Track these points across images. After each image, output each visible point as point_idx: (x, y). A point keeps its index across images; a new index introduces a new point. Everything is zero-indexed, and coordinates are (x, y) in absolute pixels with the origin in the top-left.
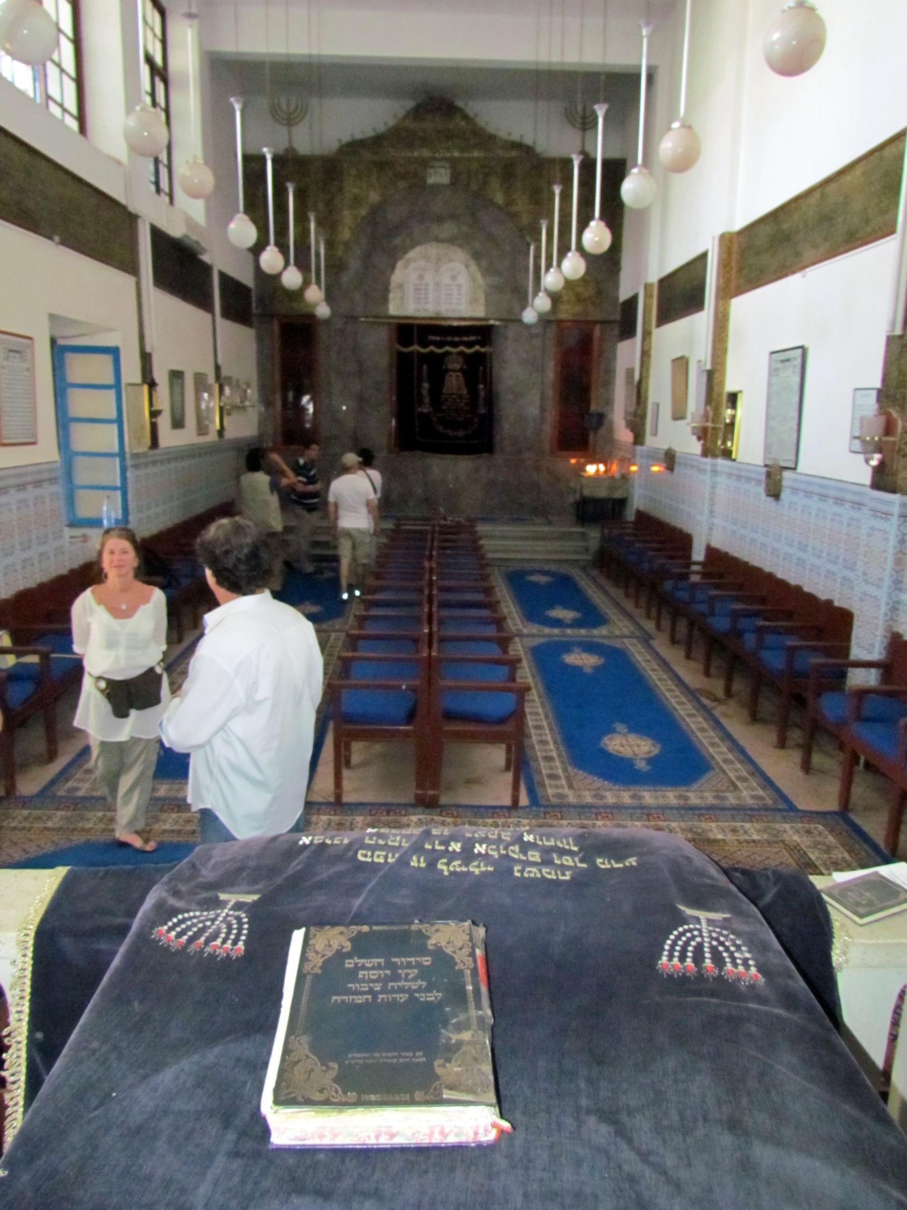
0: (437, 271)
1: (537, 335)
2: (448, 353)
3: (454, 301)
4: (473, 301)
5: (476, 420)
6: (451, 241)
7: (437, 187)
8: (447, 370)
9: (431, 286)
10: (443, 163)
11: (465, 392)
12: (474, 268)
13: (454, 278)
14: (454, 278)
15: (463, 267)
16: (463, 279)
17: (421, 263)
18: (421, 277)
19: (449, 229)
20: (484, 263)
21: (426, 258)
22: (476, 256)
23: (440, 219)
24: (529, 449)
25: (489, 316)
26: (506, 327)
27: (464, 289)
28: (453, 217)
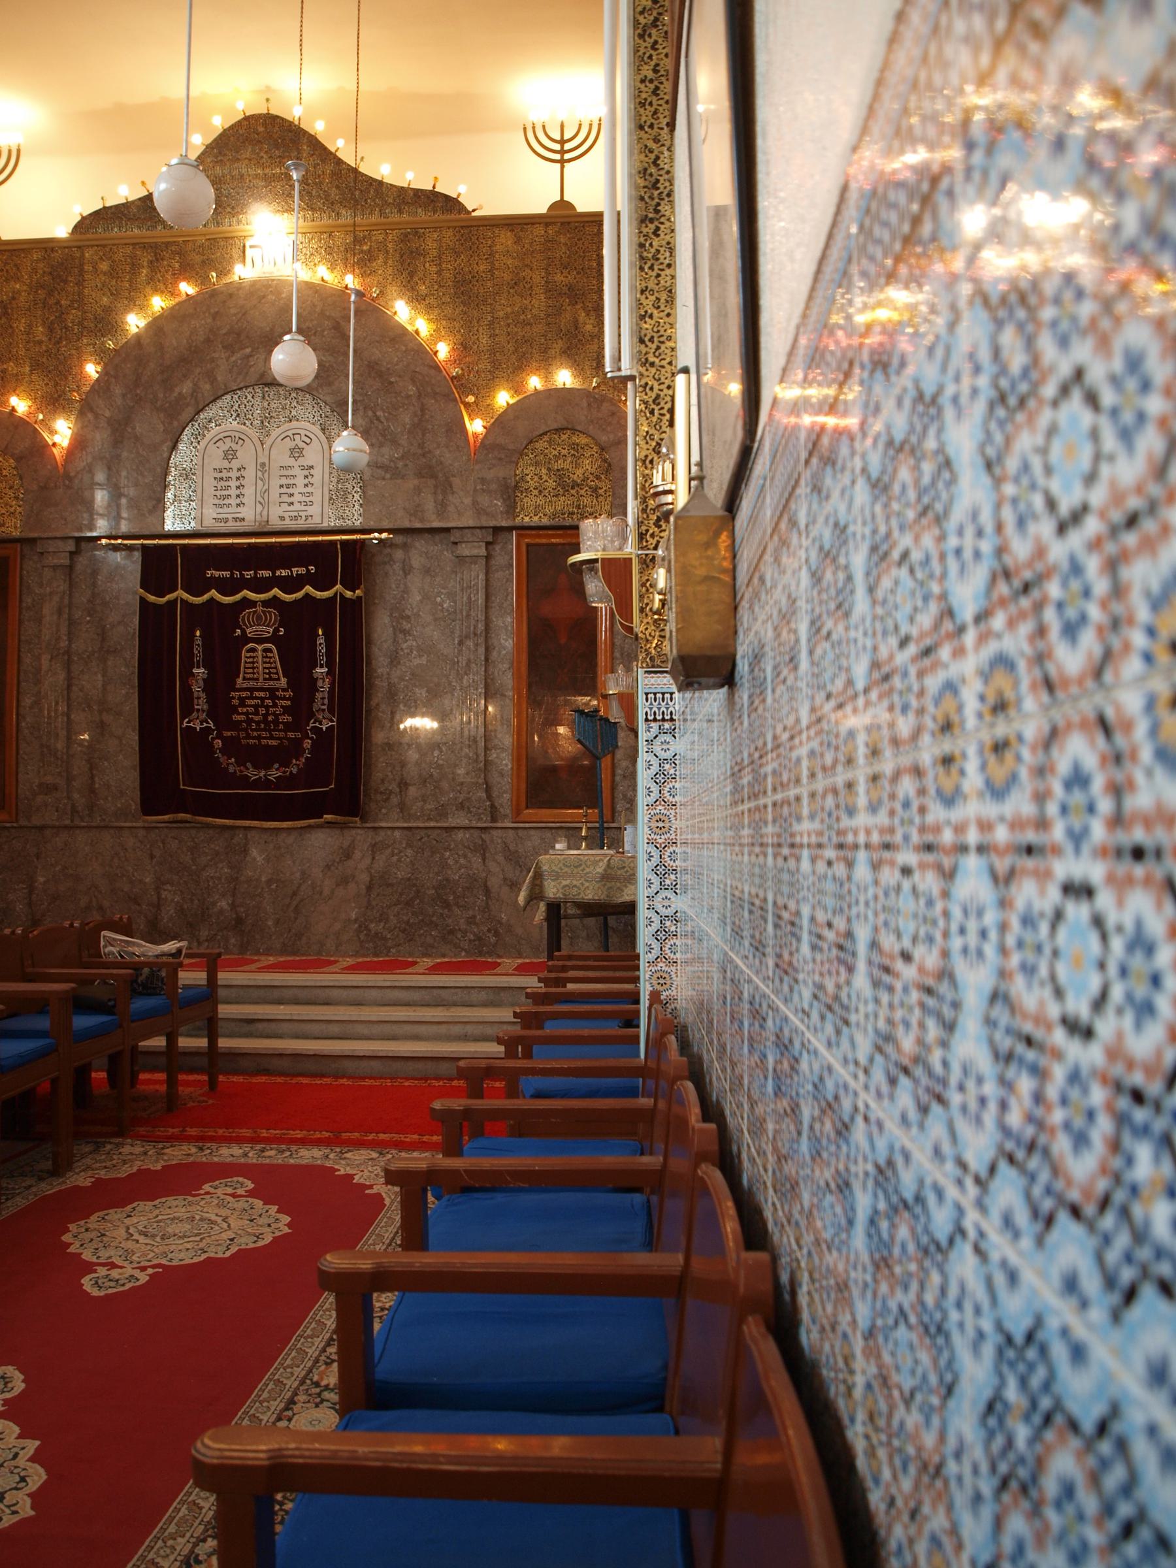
25: (372, 524)
27: (317, 472)
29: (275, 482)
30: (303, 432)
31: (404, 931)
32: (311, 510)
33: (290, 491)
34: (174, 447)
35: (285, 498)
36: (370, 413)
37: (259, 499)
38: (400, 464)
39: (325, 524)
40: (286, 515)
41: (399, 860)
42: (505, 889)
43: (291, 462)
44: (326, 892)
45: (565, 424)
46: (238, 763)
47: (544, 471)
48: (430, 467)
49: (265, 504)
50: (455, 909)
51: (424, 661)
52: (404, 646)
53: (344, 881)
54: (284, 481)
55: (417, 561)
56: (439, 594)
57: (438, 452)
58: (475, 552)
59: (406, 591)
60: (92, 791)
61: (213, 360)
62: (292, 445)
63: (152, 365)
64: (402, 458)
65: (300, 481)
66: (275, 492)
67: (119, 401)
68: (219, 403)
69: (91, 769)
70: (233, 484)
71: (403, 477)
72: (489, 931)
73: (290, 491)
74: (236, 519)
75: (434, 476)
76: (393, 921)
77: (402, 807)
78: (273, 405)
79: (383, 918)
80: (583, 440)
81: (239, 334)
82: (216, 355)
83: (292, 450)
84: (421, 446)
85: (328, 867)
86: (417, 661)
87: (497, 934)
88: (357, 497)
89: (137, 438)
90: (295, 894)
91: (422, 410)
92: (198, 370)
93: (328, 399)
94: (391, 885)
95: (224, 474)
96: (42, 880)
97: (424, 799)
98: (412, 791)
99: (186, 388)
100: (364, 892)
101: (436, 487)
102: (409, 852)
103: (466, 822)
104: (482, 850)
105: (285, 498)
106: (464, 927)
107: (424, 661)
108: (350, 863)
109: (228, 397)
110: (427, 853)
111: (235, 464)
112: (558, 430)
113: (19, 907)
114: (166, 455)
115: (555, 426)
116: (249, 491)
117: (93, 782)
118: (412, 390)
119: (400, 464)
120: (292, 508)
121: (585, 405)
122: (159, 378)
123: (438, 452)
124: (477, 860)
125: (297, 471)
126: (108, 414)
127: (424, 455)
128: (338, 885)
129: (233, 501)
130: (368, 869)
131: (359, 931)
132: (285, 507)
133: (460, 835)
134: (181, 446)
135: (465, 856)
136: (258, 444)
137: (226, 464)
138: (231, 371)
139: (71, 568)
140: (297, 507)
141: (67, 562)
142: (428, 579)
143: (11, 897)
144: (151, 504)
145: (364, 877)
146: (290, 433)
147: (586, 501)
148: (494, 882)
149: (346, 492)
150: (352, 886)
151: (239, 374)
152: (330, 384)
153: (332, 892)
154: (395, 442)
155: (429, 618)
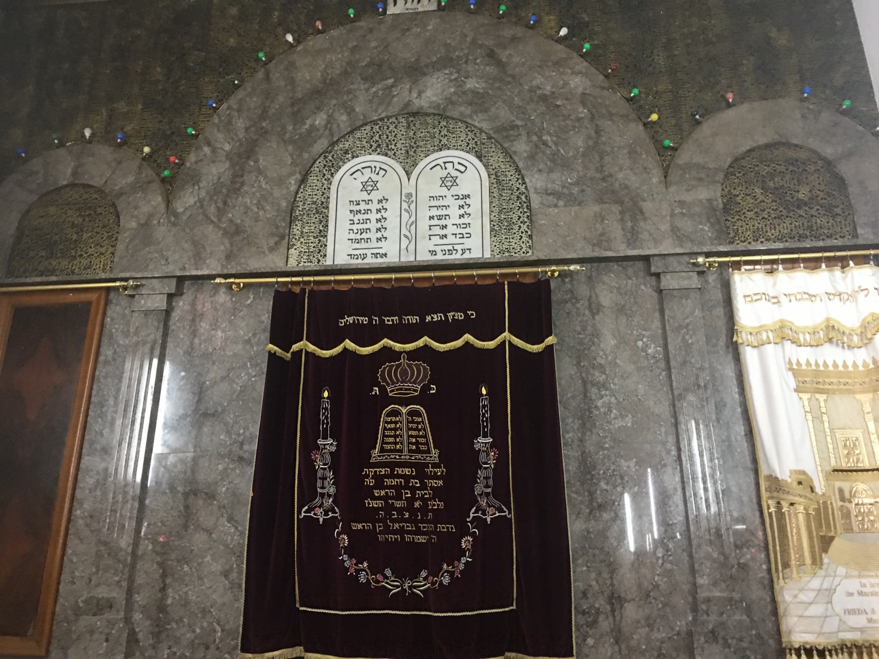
0: (408, 174)
1: (685, 292)
3: (451, 229)
4: (500, 226)
5: (466, 543)
9: (393, 206)
12: (497, 159)
13: (449, 182)
14: (449, 182)
16: (474, 179)
18: (369, 186)
23: (416, 72)
28: (447, 62)
29: (424, 214)
30: (456, 160)
32: (468, 243)
33: (443, 222)
34: (303, 181)
35: (437, 231)
36: (535, 138)
38: (575, 190)
39: (488, 255)
40: (438, 249)
43: (443, 191)
45: (777, 138)
46: (375, 569)
47: (758, 191)
48: (613, 192)
49: (414, 239)
51: (628, 421)
52: (599, 403)
54: (435, 212)
55: (606, 298)
56: (640, 337)
57: (620, 176)
58: (685, 283)
59: (596, 334)
60: (162, 608)
61: (349, 92)
62: (444, 173)
63: (281, 99)
64: (577, 184)
65: (454, 212)
66: (424, 224)
68: (358, 134)
69: (164, 576)
70: (374, 216)
71: (579, 204)
73: (443, 222)
74: (376, 255)
78: (419, 134)
80: (803, 155)
81: (380, 66)
83: (443, 180)
84: (600, 169)
86: (619, 423)
88: (524, 227)
89: (260, 172)
91: (597, 132)
92: (334, 102)
93: (485, 126)
95: (363, 207)
98: (631, 611)
99: (320, 120)
101: (622, 213)
105: (437, 231)
107: (628, 421)
109: (368, 128)
111: (375, 196)
112: (768, 146)
114: (293, 188)
115: (763, 141)
116: (392, 223)
117: (164, 597)
118: (583, 112)
119: (575, 190)
120: (445, 241)
121: (799, 116)
122: (289, 110)
123: (620, 176)
126: (227, 147)
127: (603, 179)
129: (373, 235)
132: (437, 240)
134: (312, 180)
138: (371, 101)
139: (168, 312)
140: (451, 239)
141: (164, 305)
142: (623, 320)
144: (272, 242)
146: (440, 162)
149: (511, 223)
151: (380, 104)
152: (486, 111)
155: (631, 368)
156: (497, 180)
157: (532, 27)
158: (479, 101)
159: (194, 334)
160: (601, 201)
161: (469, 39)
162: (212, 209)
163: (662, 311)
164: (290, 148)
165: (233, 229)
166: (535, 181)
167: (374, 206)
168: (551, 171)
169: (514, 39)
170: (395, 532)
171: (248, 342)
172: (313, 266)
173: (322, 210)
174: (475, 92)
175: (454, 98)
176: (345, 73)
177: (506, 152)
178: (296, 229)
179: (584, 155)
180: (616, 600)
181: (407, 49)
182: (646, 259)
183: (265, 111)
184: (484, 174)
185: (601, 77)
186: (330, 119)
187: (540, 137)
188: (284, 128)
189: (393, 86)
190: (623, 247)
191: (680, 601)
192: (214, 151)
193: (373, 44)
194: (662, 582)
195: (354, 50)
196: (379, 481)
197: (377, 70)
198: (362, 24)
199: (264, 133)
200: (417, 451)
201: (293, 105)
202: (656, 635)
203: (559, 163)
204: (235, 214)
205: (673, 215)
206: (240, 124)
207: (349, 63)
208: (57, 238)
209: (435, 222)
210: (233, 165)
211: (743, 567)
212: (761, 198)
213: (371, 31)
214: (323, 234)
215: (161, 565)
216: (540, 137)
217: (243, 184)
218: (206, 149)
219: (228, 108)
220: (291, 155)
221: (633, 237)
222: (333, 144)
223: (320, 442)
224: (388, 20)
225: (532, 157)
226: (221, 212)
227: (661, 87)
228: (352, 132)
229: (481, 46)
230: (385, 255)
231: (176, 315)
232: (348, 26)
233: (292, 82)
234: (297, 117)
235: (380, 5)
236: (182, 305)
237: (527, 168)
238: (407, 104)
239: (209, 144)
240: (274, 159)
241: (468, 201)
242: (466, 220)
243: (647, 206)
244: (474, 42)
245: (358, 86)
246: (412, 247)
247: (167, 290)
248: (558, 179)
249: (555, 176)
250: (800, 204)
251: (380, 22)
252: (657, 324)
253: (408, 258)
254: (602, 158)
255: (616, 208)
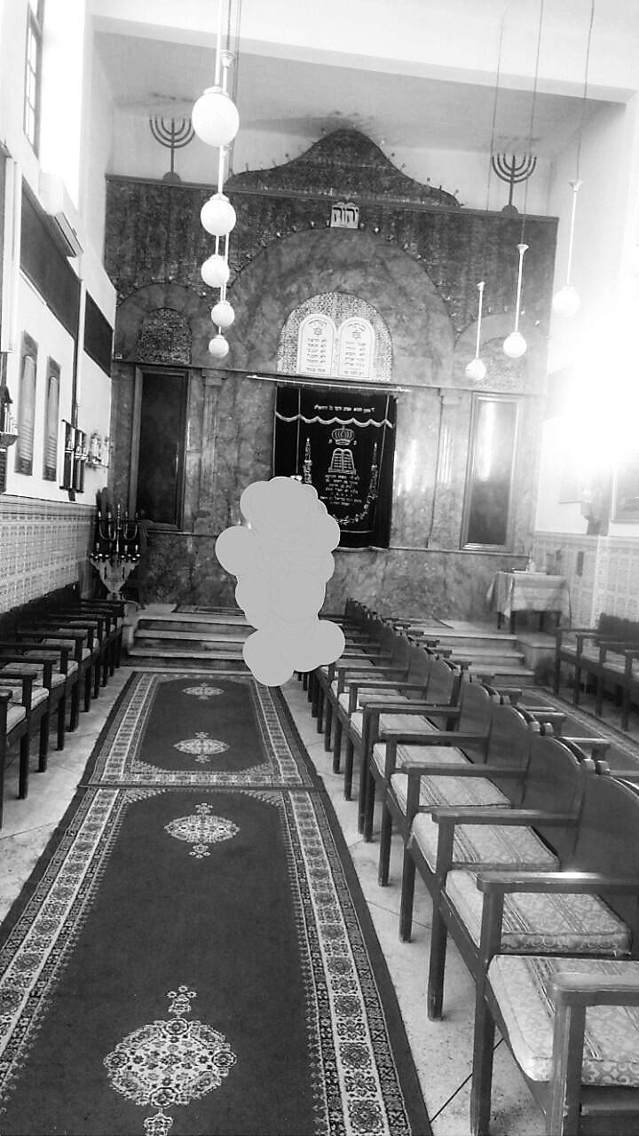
1: (451, 407)
2: (336, 425)
3: (355, 362)
4: (379, 362)
6: (356, 293)
7: (345, 232)
8: (334, 446)
10: (349, 205)
11: (354, 472)
12: (380, 325)
15: (368, 322)
17: (321, 316)
18: (318, 332)
19: (353, 279)
20: (392, 320)
21: (325, 310)
22: (384, 311)
23: (344, 266)
24: (435, 540)
25: (396, 381)
26: (414, 396)
28: (360, 265)
31: (400, 604)
32: (363, 369)
34: (285, 323)
37: (334, 359)
41: (400, 566)
42: (455, 585)
44: (360, 581)
47: (491, 361)
50: (428, 593)
53: (370, 576)
55: (419, 404)
56: (430, 424)
58: (452, 402)
61: (310, 274)
62: (354, 330)
63: (273, 272)
64: (415, 345)
67: (253, 291)
68: (312, 299)
69: (229, 504)
72: (445, 605)
75: (432, 357)
76: (395, 597)
77: (402, 538)
79: (390, 596)
82: (312, 271)
84: (426, 338)
85: (362, 568)
87: (449, 608)
90: (343, 580)
92: (301, 279)
93: (376, 305)
94: (394, 579)
95: (314, 342)
96: (199, 565)
97: (414, 534)
98: (408, 530)
99: (294, 288)
100: (380, 582)
102: (406, 562)
103: (437, 549)
104: (444, 563)
105: (348, 361)
106: (432, 603)
108: (374, 566)
109: (318, 296)
110: (415, 563)
113: (183, 580)
114: (280, 327)
116: (328, 353)
118: (423, 306)
119: (414, 348)
122: (277, 280)
124: (441, 568)
125: (356, 345)
126: (246, 298)
128: (366, 577)
130: (384, 570)
131: (376, 602)
133: (433, 555)
135: (435, 566)
136: (334, 326)
137: (315, 337)
143: (178, 574)
145: (381, 574)
147: (512, 379)
148: (450, 581)
150: (374, 579)
152: (377, 297)
153: (363, 581)
154: (412, 336)
156: (379, 335)
157: (404, 250)
158: (375, 291)
159: (235, 399)
160: (424, 355)
161: (373, 252)
162: (239, 334)
163: (441, 413)
164: (279, 303)
165: (249, 345)
166: (397, 340)
167: (320, 343)
168: (404, 336)
169: (395, 257)
170: (337, 501)
171: (259, 407)
172: (291, 373)
173: (294, 341)
174: (373, 284)
175: (363, 287)
176: (308, 262)
177: (386, 323)
178: (281, 349)
179: (420, 330)
180: (404, 527)
181: (341, 251)
182: (439, 389)
183: (265, 277)
184: (373, 333)
185: (434, 287)
186: (299, 288)
187: (401, 317)
188: (276, 292)
189: (332, 274)
190: (430, 381)
191: (426, 528)
192: (239, 299)
193: (323, 246)
194: (422, 521)
195: (313, 247)
196: (332, 481)
197: (324, 263)
198: (317, 231)
199: (265, 292)
200: (347, 469)
201: (280, 277)
202: (416, 539)
203: (408, 332)
204: (251, 337)
205: (454, 368)
206: (253, 285)
207: (310, 255)
208: (160, 338)
209: (348, 356)
210: (249, 310)
211: (450, 517)
212: (492, 364)
213: (322, 237)
214: (294, 355)
215: (227, 500)
216: (401, 317)
217: (255, 320)
218: (235, 298)
219: (246, 274)
220: (279, 307)
221: (435, 377)
222: (301, 303)
223: (306, 461)
224: (332, 230)
225: (396, 327)
226: (244, 335)
227: (460, 297)
228: (310, 298)
229: (378, 257)
230: (324, 370)
231: (225, 388)
232: (310, 231)
233: (279, 263)
234: (283, 286)
235: (328, 222)
236: (228, 383)
237: (394, 332)
238: (338, 287)
239: (236, 294)
240: (270, 307)
241: (364, 347)
242: (362, 357)
243: (444, 361)
244: (375, 255)
245: (314, 271)
246: (337, 368)
247: (222, 377)
248: (408, 341)
249: (405, 339)
250: (507, 369)
251: (328, 232)
252: (438, 419)
253: (334, 376)
254: (428, 333)
255: (430, 360)
